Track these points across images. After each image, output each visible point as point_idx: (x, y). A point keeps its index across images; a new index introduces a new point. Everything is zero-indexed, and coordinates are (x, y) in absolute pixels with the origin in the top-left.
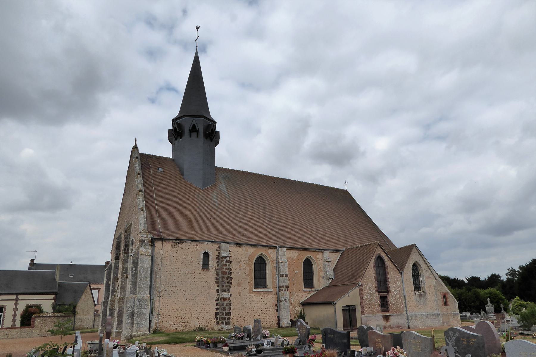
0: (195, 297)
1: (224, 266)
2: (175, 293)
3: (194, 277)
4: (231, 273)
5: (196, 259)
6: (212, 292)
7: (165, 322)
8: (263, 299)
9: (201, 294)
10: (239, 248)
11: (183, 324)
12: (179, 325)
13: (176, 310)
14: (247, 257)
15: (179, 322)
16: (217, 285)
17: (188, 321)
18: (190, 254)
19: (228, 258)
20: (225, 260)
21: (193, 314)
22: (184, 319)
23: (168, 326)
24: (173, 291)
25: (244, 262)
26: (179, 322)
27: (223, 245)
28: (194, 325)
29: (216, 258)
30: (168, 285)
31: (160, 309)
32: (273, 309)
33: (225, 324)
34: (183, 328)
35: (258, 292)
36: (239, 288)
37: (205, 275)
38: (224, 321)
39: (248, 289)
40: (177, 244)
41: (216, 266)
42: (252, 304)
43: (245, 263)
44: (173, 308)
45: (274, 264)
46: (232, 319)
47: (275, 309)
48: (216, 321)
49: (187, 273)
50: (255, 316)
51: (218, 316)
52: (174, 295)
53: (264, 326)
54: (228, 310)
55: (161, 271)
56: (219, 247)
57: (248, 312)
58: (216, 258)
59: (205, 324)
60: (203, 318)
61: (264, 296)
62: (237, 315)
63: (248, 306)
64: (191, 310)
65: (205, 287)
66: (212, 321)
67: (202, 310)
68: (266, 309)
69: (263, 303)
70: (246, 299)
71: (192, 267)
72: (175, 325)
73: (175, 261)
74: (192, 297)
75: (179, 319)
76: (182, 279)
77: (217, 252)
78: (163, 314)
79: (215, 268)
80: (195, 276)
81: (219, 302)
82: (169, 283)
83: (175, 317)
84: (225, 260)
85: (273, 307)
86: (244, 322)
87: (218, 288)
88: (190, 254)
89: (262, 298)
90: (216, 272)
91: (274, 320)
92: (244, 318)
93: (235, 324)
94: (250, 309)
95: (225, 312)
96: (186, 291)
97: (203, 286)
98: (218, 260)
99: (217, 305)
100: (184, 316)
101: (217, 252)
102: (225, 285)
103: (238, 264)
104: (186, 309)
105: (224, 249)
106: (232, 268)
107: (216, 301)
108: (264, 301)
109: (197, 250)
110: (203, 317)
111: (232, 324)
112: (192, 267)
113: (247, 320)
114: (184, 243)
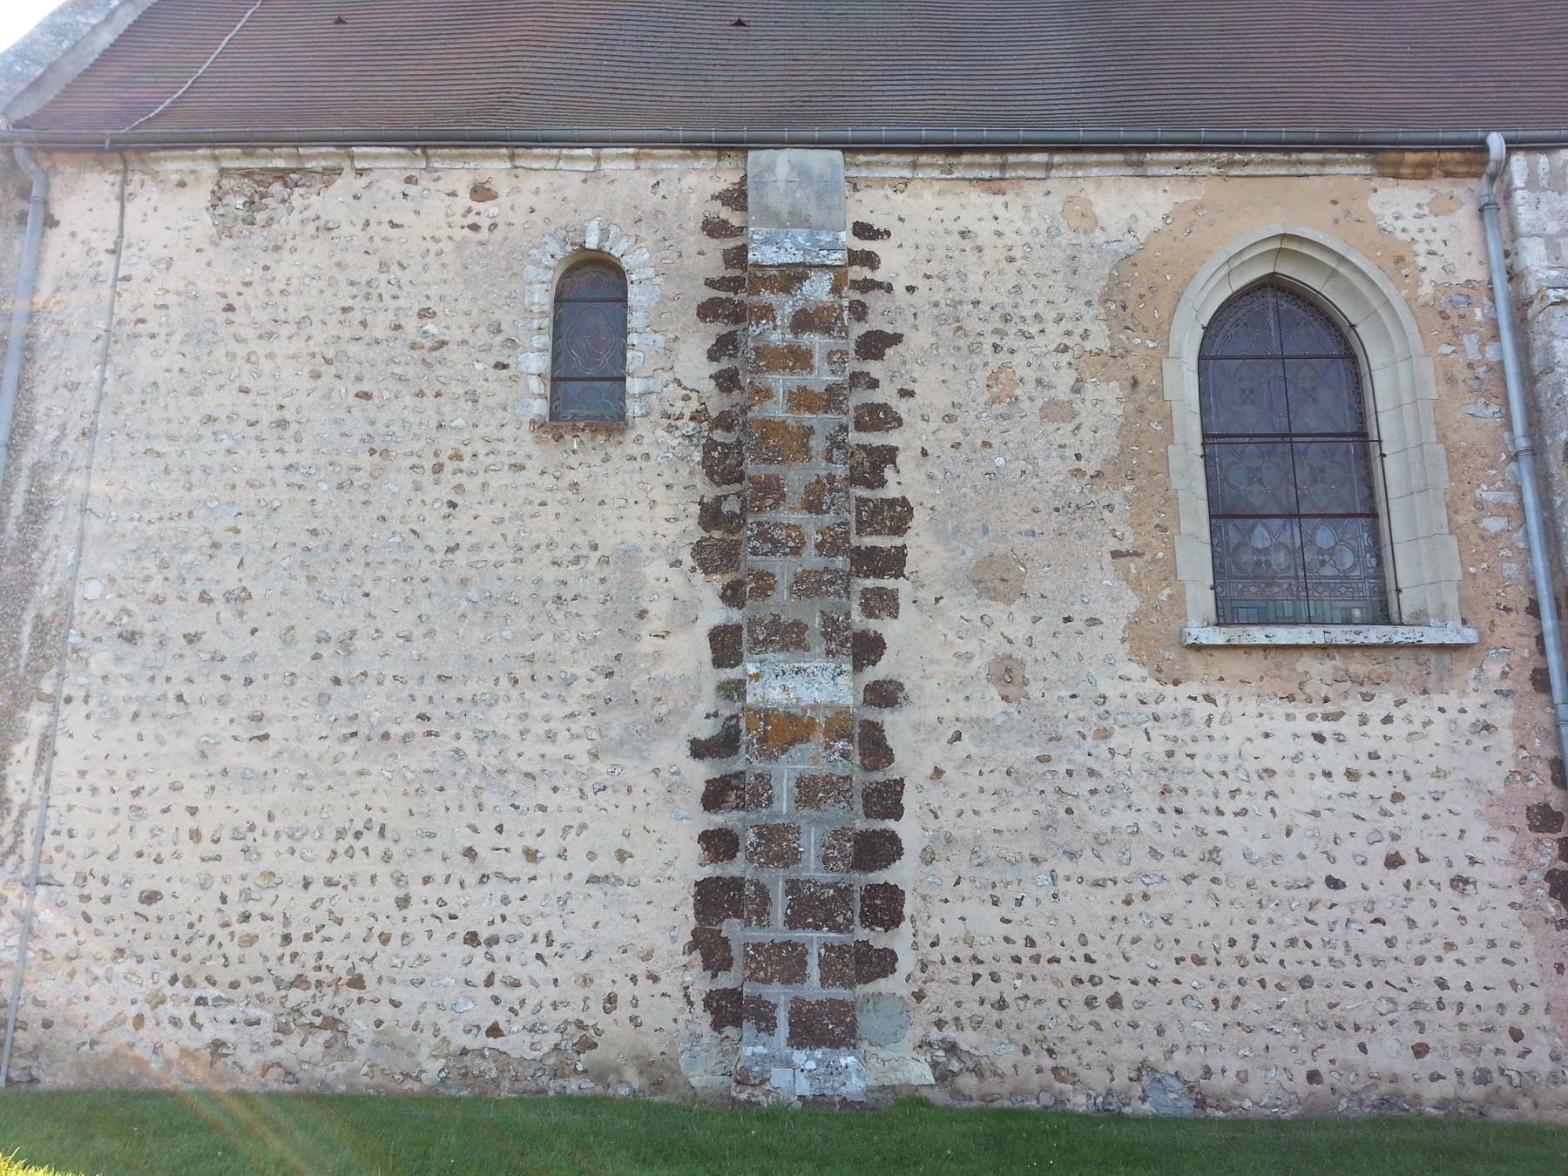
0: (457, 709)
1: (770, 368)
2: (225, 668)
3: (453, 505)
4: (889, 455)
5: (475, 328)
6: (657, 656)
7: (98, 971)
8: (1340, 738)
9: (523, 672)
10: (988, 198)
11: (296, 996)
12: (254, 1012)
13: (229, 847)
14: (1094, 285)
15: (258, 979)
16: (719, 580)
17: (362, 968)
18: (405, 276)
19: (818, 289)
20: (786, 306)
21: (417, 890)
22: (315, 946)
23: (132, 1012)
24: (213, 640)
25: (1055, 334)
26: (258, 979)
27: (770, 168)
28: (424, 1019)
29: (707, 311)
30: (155, 587)
31: (52, 824)
32: (1510, 874)
33: (783, 1029)
34: (290, 1050)
35: (1258, 656)
36: (996, 610)
37: (572, 476)
38: (778, 994)
39: (1113, 627)
40: (277, 188)
41: (709, 386)
42: (1188, 803)
43: (1065, 349)
44: (189, 823)
45: (1470, 343)
46: (924, 967)
47: (1535, 876)
48: (701, 983)
49: (365, 460)
50: (1244, 944)
51: (731, 928)
52: (218, 687)
53: (1385, 1088)
54: (826, 860)
55: (91, 452)
56: (736, 198)
57: (1137, 888)
58: (707, 311)
59: (569, 1014)
60: (540, 947)
61: (1354, 707)
62: (985, 921)
63: (1123, 819)
64: (406, 843)
65: (573, 607)
66: (654, 978)
67: (531, 855)
68: (1393, 862)
69: (1348, 787)
70: (1104, 734)
71: (429, 402)
72: (201, 1001)
73: (242, 351)
74: (421, 706)
75: (250, 940)
76: (314, 525)
77: (716, 248)
78: (82, 879)
79: (694, 405)
80: (459, 488)
81: (737, 764)
82: (164, 565)
83: (210, 925)
84: (786, 306)
85: (1502, 848)
86: (1086, 1016)
87: (736, 616)
88: (405, 276)
89: (1326, 728)
90: (710, 445)
91: (1537, 1012)
92: (1084, 970)
93: (966, 1039)
94: (1154, 853)
95: (793, 887)
96: (358, 643)
97: (552, 591)
98: (720, 328)
99: (714, 797)
100: (321, 915)
101: (716, 248)
102: (783, 569)
103: (977, 360)
104: (341, 834)
105: (784, 208)
106: (901, 407)
107: (699, 750)
108: (1363, 765)
109: (484, 234)
110: (540, 926)
111: (915, 1034)
112: (429, 402)
113: (1124, 988)
114: (337, 171)
